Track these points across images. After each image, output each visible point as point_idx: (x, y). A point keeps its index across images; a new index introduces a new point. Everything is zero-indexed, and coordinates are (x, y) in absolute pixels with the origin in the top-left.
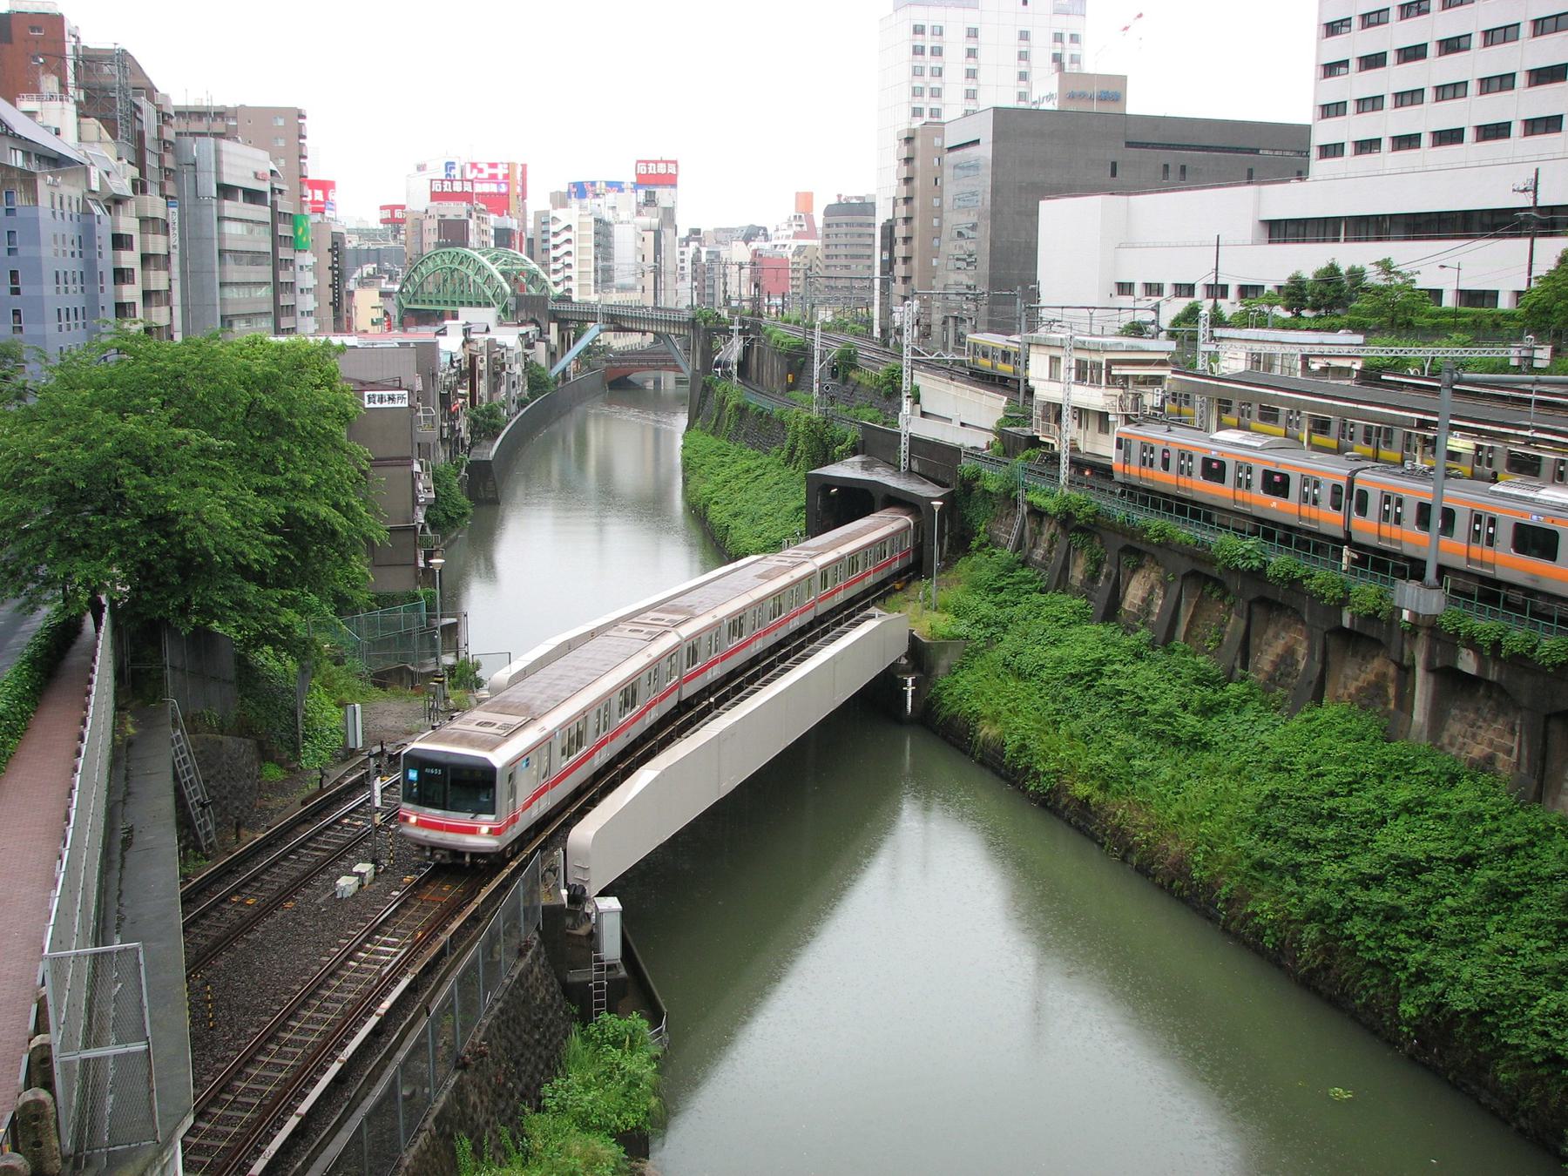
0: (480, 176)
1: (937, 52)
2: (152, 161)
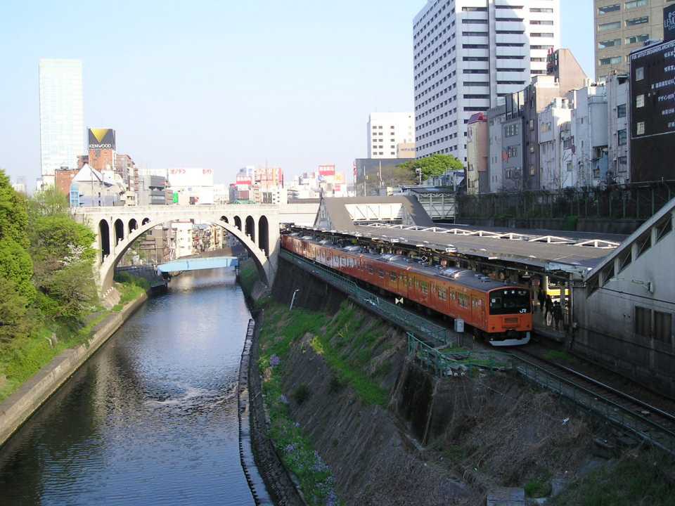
2: (132, 182)
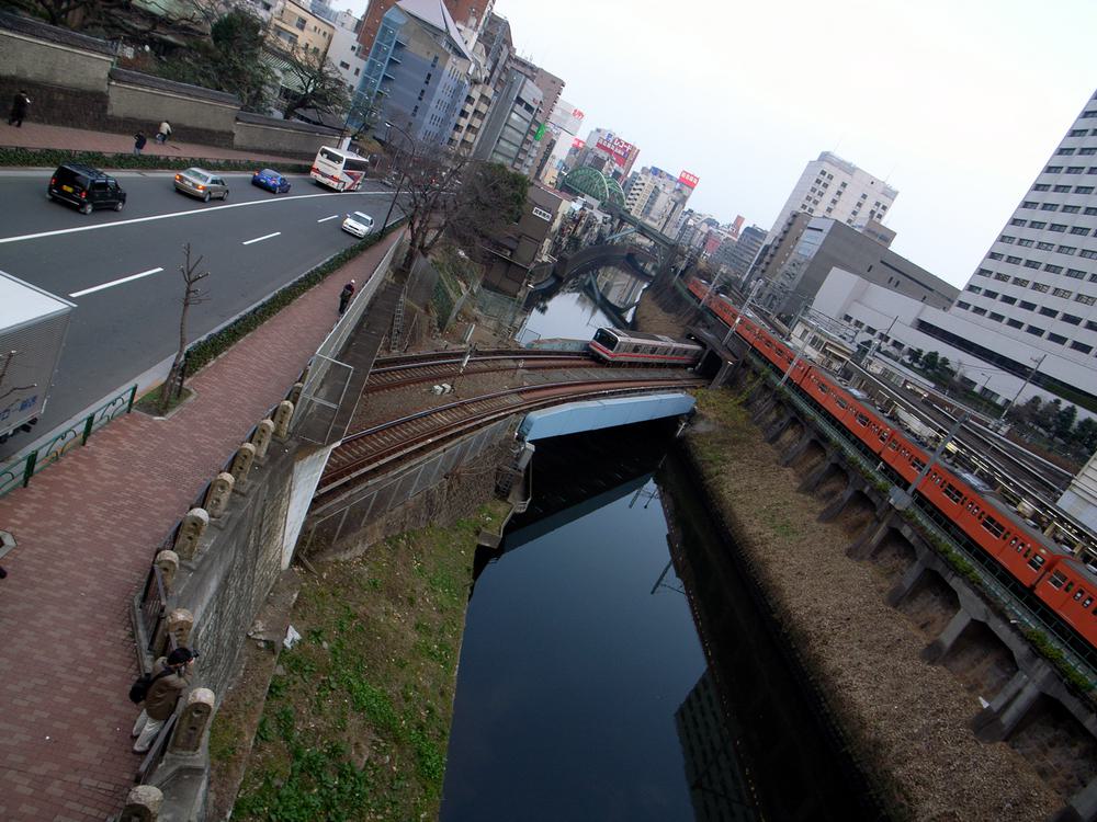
1: (826, 186)
2: (496, 74)
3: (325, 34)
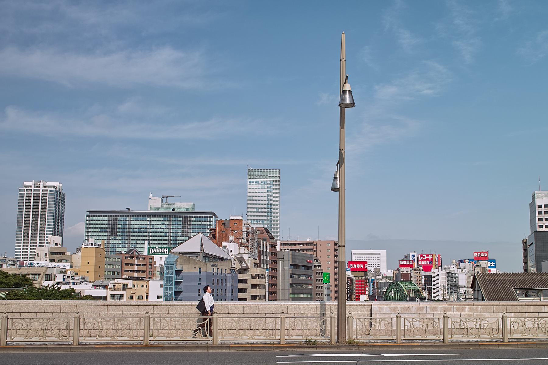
0: (423, 259)
3: (142, 286)
